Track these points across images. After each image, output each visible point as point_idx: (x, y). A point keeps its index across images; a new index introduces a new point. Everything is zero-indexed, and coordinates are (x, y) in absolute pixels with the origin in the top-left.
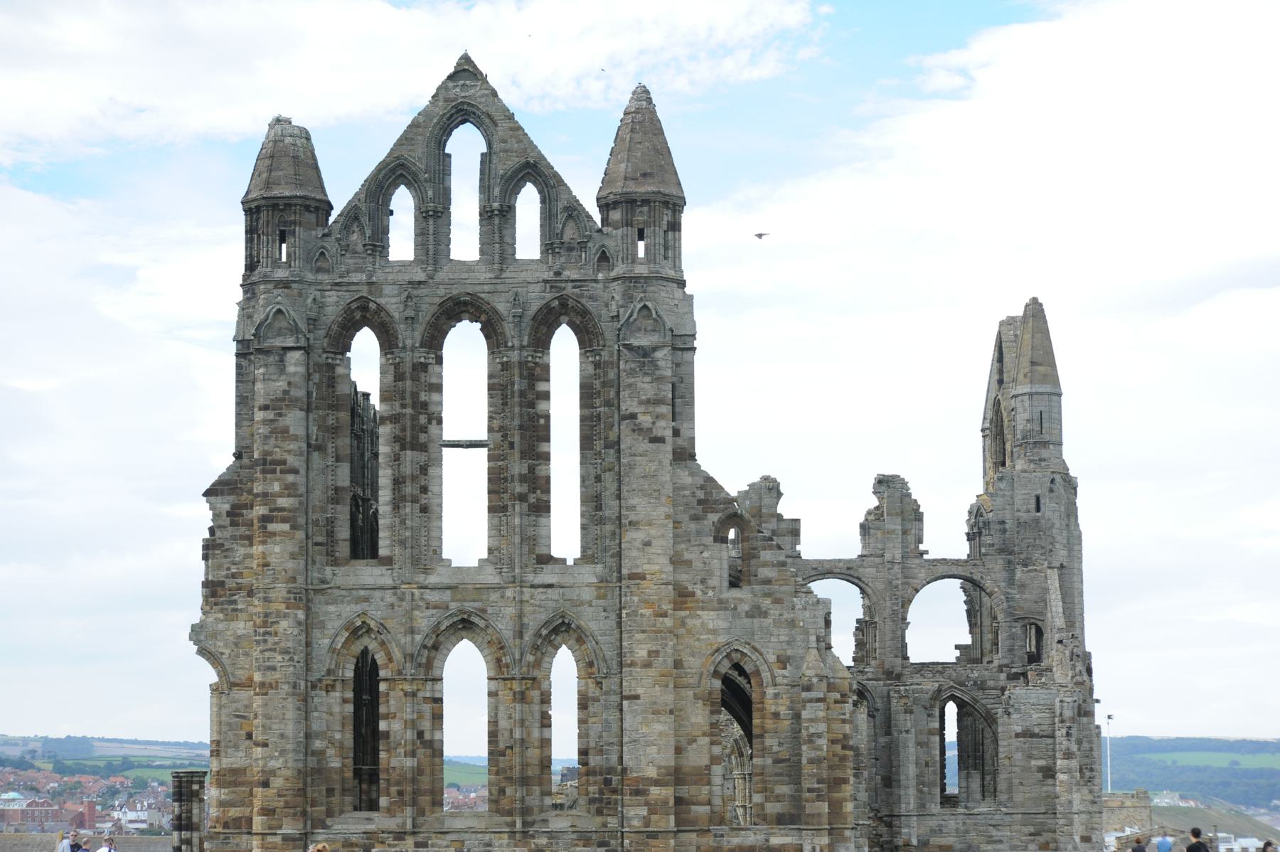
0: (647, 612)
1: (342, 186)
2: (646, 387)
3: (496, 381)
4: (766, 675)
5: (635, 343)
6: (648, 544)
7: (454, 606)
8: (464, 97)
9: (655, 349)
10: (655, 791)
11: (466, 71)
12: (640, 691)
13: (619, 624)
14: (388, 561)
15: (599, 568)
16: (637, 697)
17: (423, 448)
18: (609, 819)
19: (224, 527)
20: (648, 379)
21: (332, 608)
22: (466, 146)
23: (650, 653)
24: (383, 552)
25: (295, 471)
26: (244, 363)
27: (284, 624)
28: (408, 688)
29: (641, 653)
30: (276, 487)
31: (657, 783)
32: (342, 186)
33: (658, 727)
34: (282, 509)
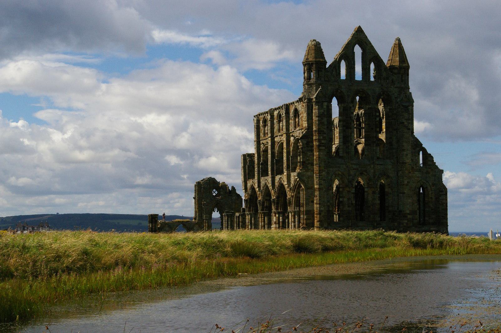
0: (407, 172)
1: (330, 59)
2: (406, 115)
3: (366, 112)
4: (429, 188)
5: (404, 104)
6: (407, 155)
7: (360, 169)
8: (359, 37)
9: (408, 106)
10: (409, 216)
11: (359, 31)
12: (405, 192)
13: (397, 175)
14: (341, 157)
15: (392, 161)
16: (405, 193)
17: (351, 129)
18: (395, 223)
19: (305, 147)
20: (407, 114)
21: (331, 169)
22: (358, 50)
23: (407, 182)
24: (341, 155)
25: (325, 134)
26: (309, 104)
27: (324, 173)
28: (348, 189)
29: (406, 182)
30: (321, 138)
31: (409, 214)
32: (330, 59)
33: (410, 201)
34: (323, 143)
